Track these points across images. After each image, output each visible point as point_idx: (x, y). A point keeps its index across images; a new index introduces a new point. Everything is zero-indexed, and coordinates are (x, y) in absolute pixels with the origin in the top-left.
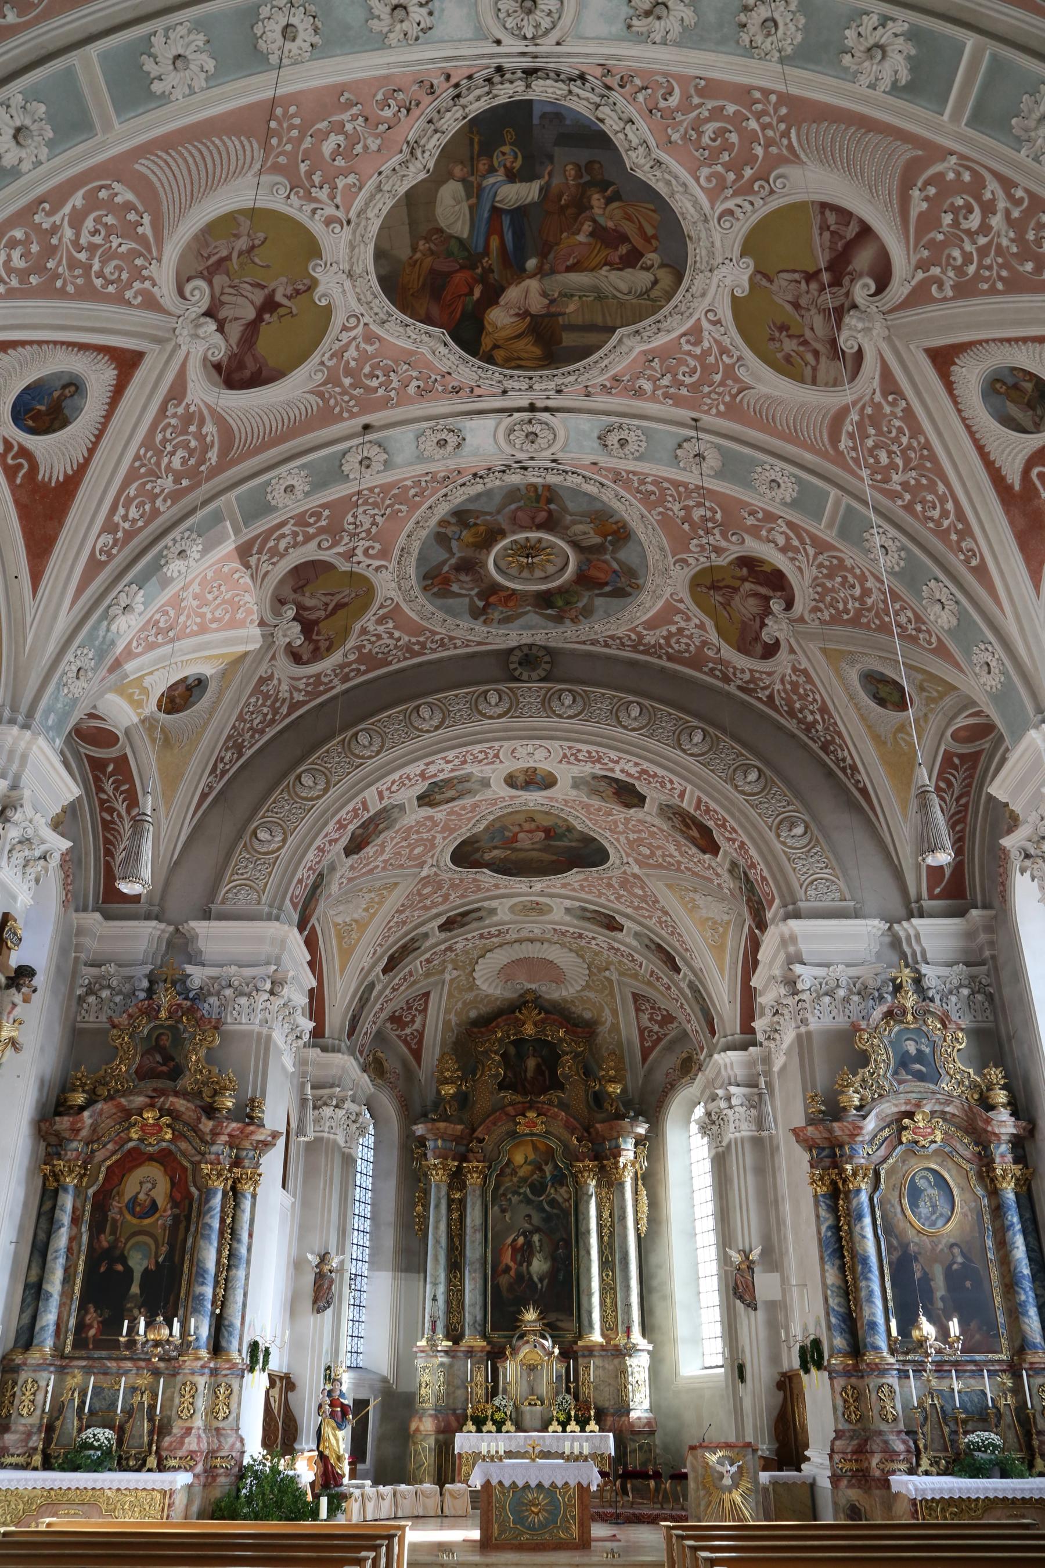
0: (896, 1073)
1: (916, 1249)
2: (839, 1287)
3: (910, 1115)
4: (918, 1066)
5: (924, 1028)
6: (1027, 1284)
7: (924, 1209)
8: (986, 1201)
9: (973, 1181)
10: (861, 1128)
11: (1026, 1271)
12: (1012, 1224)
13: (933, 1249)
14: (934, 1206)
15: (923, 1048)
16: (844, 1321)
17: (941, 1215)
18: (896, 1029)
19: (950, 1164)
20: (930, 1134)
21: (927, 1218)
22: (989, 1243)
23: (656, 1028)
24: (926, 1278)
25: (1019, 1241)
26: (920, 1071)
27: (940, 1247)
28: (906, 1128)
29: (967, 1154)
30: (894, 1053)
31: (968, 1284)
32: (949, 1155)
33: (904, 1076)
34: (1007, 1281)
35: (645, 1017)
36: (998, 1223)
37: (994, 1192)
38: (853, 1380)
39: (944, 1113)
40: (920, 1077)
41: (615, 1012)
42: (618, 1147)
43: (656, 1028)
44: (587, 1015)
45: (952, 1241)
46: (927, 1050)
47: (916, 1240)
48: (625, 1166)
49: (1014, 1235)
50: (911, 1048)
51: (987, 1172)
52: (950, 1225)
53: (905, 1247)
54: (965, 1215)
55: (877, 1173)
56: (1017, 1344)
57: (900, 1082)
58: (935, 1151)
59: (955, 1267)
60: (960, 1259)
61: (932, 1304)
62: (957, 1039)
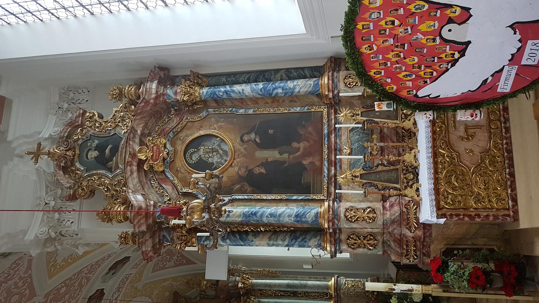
0: (110, 170)
1: (243, 170)
2: (270, 239)
3: (141, 163)
4: (107, 151)
5: (80, 142)
6: (270, 86)
7: (215, 159)
8: (211, 110)
9: (196, 118)
10: (140, 208)
11: (261, 85)
12: (226, 92)
13: (244, 156)
14: (213, 150)
15: (94, 145)
16: (296, 238)
17: (219, 145)
18: (78, 165)
19: (182, 135)
20: (158, 148)
21: (221, 157)
22: (242, 111)
23: (176, 257)
24: (265, 164)
25: (237, 88)
26: (111, 149)
27: (242, 150)
28: (151, 167)
29: (176, 120)
30: (95, 170)
31: (271, 132)
32: (176, 134)
33: (112, 164)
34: (270, 101)
35: (168, 264)
36: (229, 103)
37: (205, 103)
38: (343, 237)
39: (143, 135)
40: (115, 151)
41: (165, 280)
42: (232, 286)
43: (176, 257)
44: (167, 294)
45: (238, 140)
46: (96, 142)
47: (236, 169)
48: (243, 283)
49: (233, 91)
50: (93, 154)
51: (188, 106)
52: (227, 140)
53: (241, 179)
54: (220, 128)
55: (185, 195)
56: (316, 99)
57: (117, 167)
58: (172, 146)
59: (258, 140)
60: (253, 136)
61: (285, 162)
62: (91, 118)
